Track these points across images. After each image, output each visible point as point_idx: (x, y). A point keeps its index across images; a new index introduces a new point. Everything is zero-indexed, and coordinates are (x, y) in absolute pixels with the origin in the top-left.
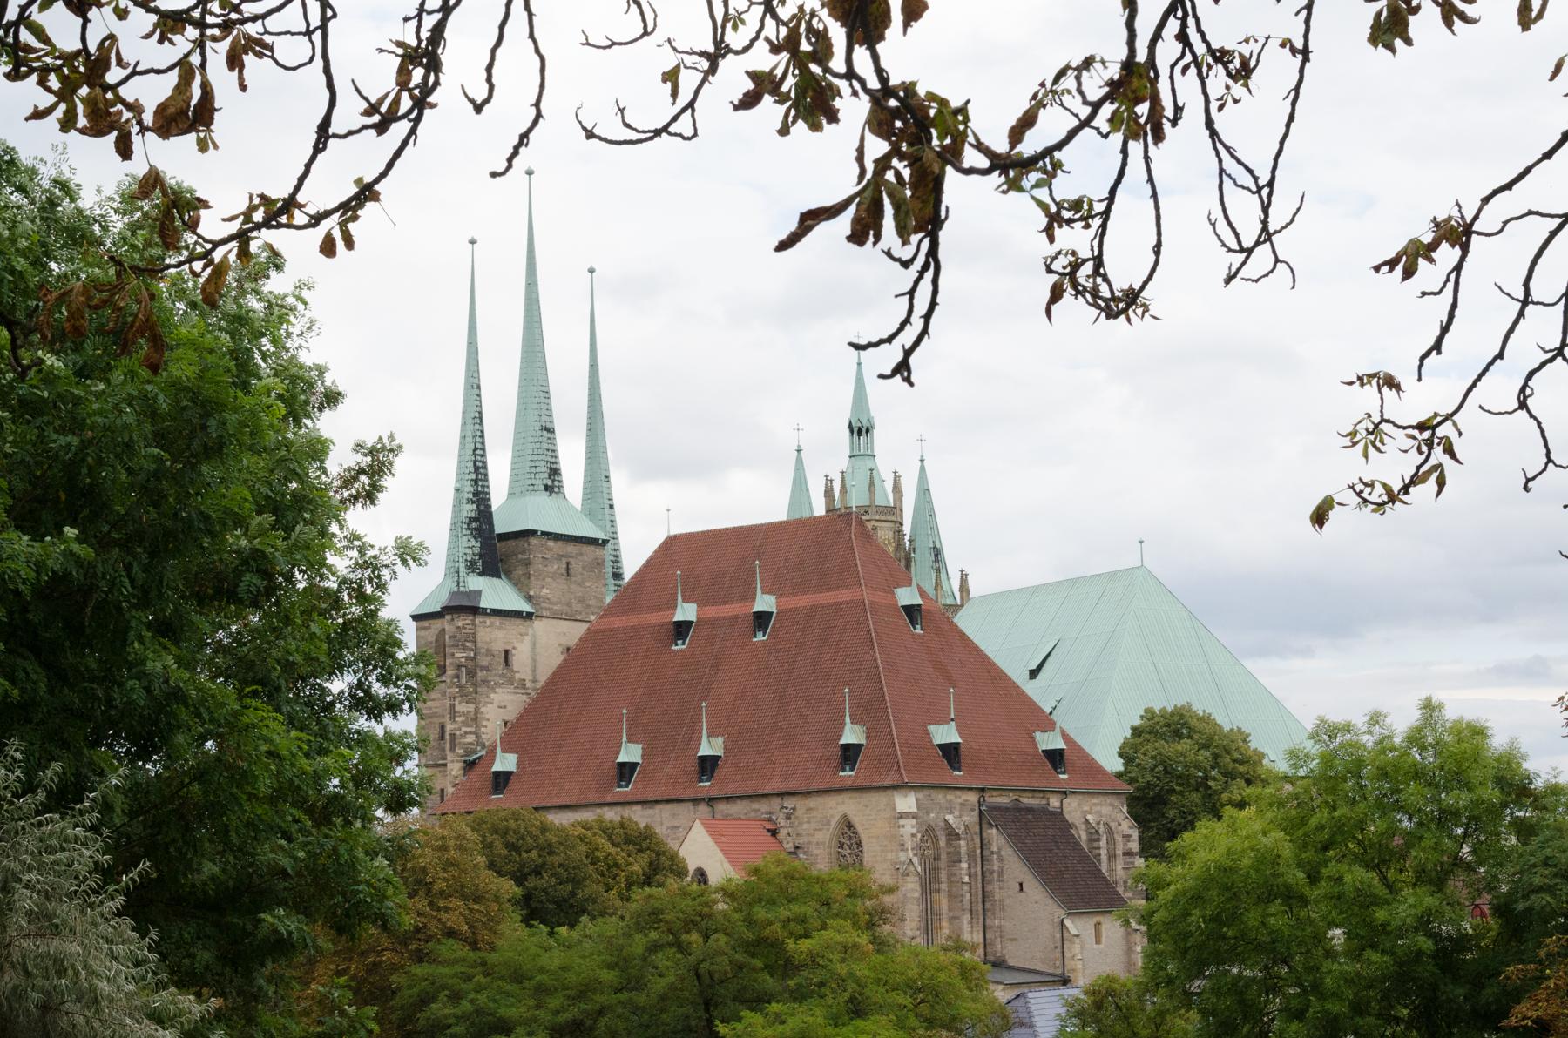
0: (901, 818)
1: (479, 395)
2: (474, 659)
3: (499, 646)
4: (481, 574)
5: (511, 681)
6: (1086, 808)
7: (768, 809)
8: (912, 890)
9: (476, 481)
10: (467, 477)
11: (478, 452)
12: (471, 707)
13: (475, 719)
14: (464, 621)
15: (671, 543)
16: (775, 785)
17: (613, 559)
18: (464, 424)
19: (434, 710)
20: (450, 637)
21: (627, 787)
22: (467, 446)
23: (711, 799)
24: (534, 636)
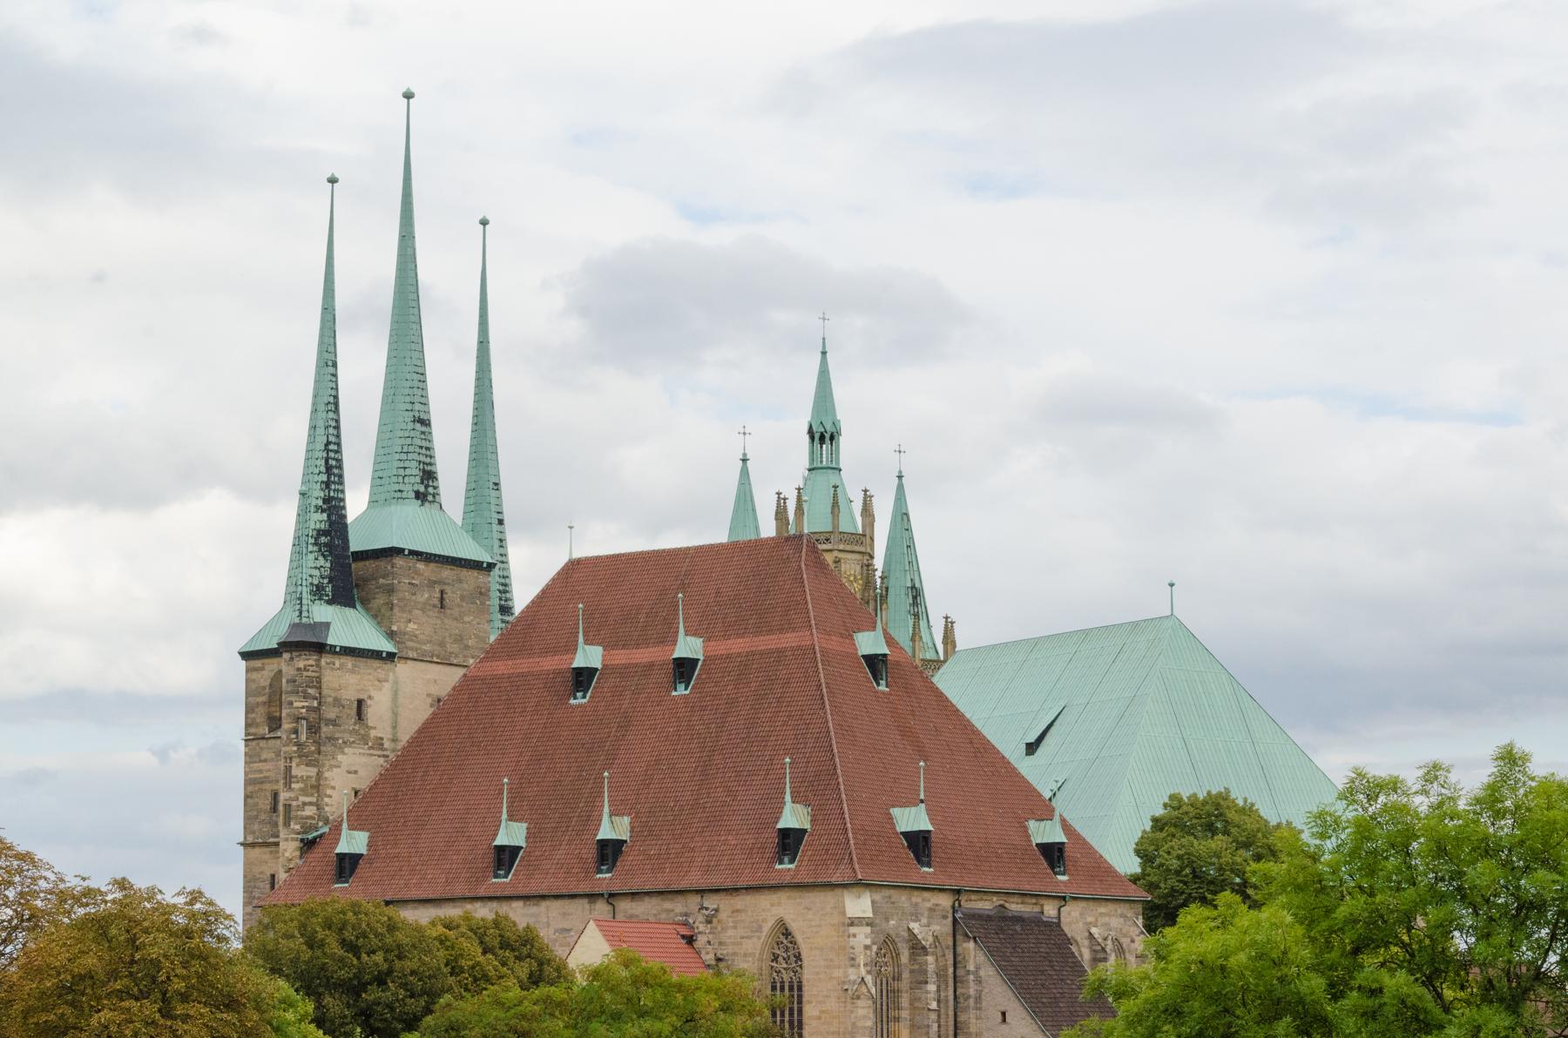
0: (852, 924)
1: (335, 375)
2: (317, 710)
3: (350, 695)
4: (330, 602)
5: (364, 739)
6: (1090, 919)
7: (684, 910)
8: (864, 1017)
9: (327, 484)
10: (316, 478)
11: (332, 447)
12: (312, 771)
13: (317, 787)
14: (305, 661)
15: (574, 568)
16: (695, 879)
17: (501, 588)
18: (315, 411)
20: (288, 681)
21: (507, 878)
22: (317, 438)
23: (612, 895)
24: (396, 682)
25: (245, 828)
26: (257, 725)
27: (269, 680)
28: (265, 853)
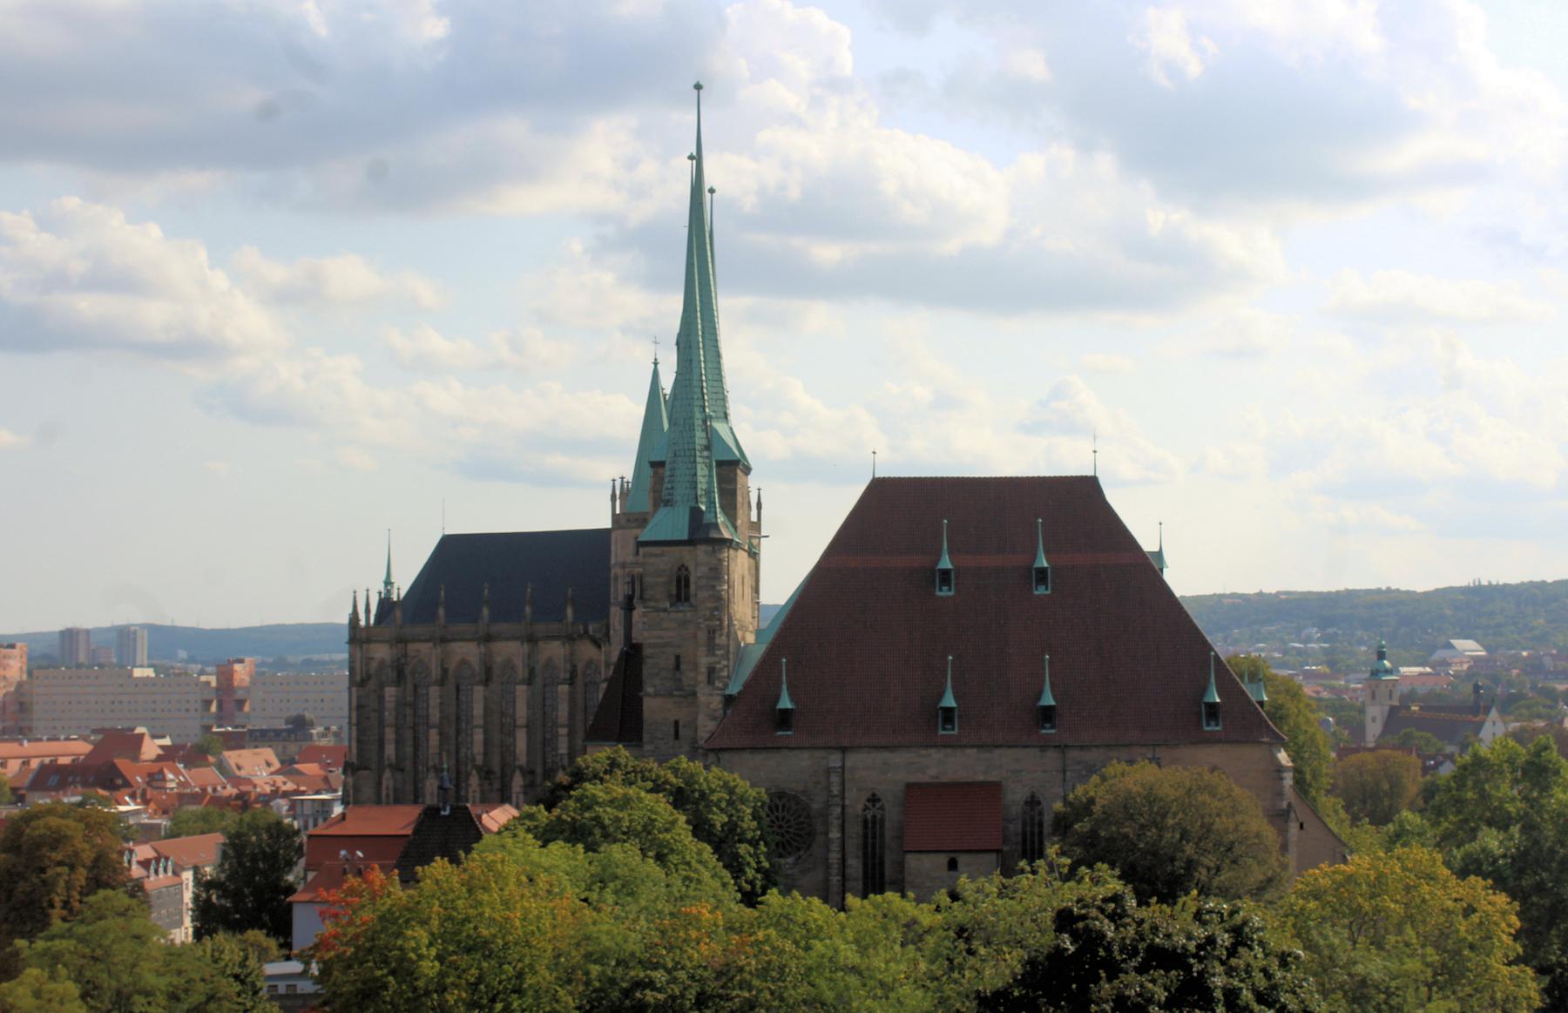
20: (710, 569)
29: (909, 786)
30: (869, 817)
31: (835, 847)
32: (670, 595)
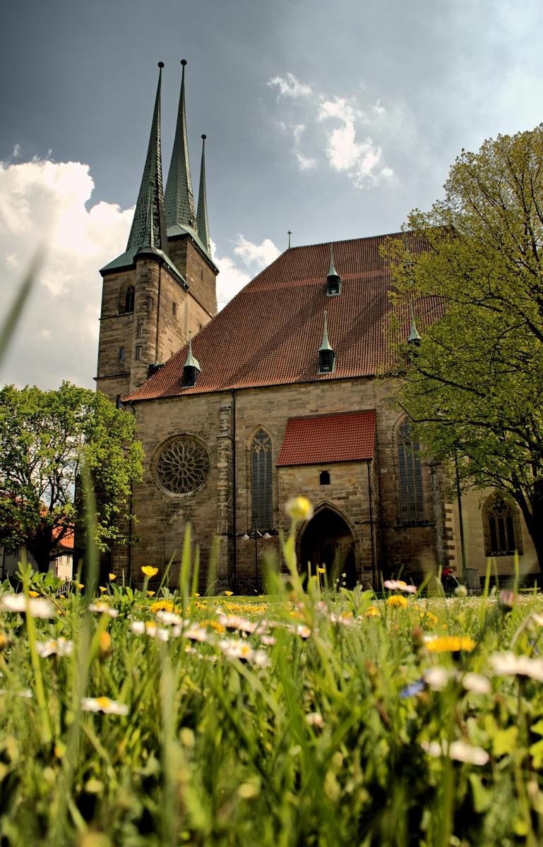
5: (175, 325)
19: (115, 337)
20: (142, 276)
25: (98, 369)
26: (111, 310)
27: (120, 285)
28: (113, 383)
29: (292, 421)
30: (257, 451)
31: (223, 475)
32: (120, 306)
